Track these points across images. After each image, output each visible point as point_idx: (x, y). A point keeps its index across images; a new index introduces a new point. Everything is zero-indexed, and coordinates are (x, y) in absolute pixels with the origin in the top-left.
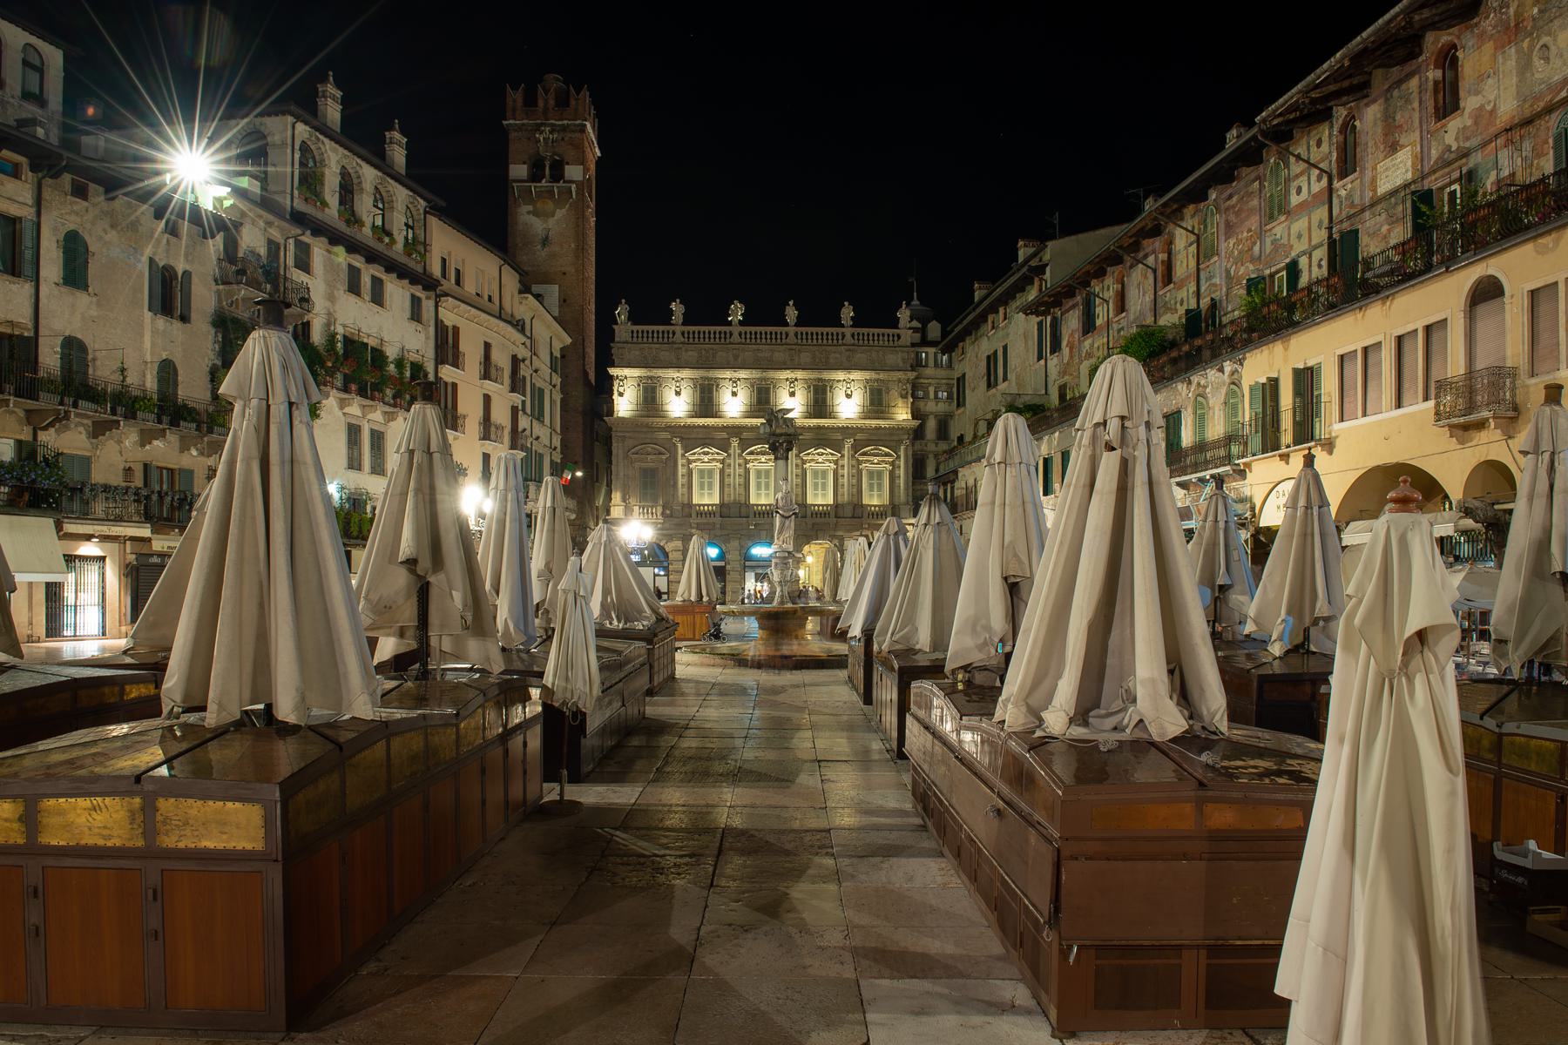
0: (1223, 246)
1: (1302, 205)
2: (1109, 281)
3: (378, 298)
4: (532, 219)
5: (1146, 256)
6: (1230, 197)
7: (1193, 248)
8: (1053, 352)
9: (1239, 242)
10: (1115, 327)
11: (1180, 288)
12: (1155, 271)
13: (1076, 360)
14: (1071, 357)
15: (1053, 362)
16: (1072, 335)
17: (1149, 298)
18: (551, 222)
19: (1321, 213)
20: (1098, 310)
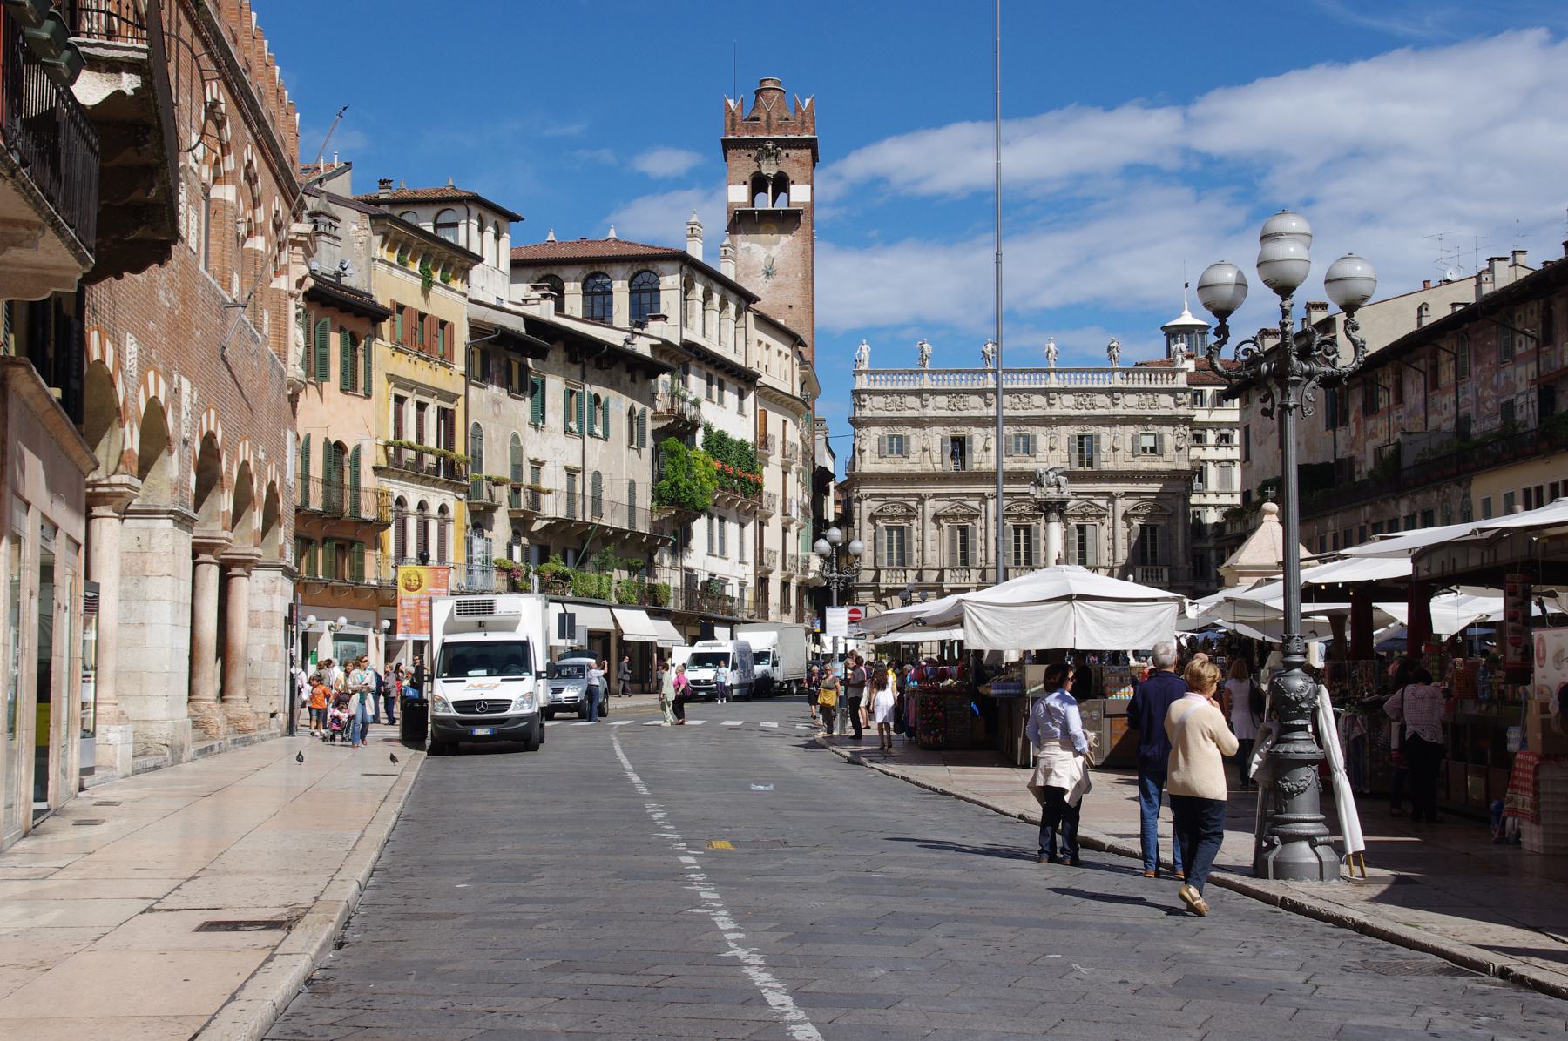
0: (1473, 370)
1: (1522, 355)
2: (1389, 370)
3: (721, 401)
4: (755, 247)
5: (1418, 359)
6: (1477, 331)
7: (1452, 364)
9: (1483, 370)
10: (1395, 414)
11: (1444, 394)
12: (1425, 374)
14: (1358, 432)
17: (1421, 396)
18: (775, 251)
19: (1532, 367)
20: (1381, 394)
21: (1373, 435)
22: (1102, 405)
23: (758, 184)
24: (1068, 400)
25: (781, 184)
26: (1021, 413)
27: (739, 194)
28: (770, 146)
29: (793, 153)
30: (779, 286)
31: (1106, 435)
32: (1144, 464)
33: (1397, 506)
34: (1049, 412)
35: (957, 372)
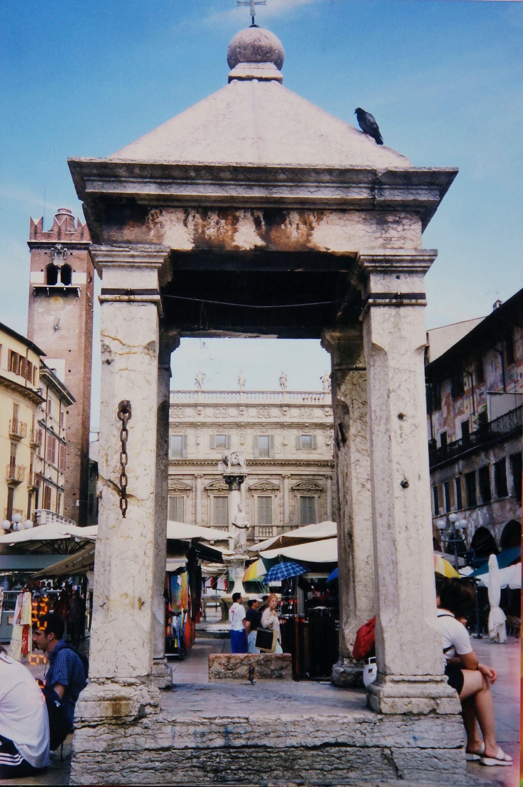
8: (435, 410)
10: (478, 391)
12: (502, 354)
13: (452, 413)
15: (436, 417)
16: (447, 397)
17: (500, 371)
20: (465, 380)
21: (461, 412)
22: (276, 415)
23: (51, 272)
24: (253, 411)
25: (67, 273)
26: (221, 420)
27: (40, 279)
28: (59, 247)
29: (75, 252)
30: (62, 338)
31: (279, 435)
32: (303, 456)
33: (487, 456)
34: (240, 419)
35: (179, 392)
